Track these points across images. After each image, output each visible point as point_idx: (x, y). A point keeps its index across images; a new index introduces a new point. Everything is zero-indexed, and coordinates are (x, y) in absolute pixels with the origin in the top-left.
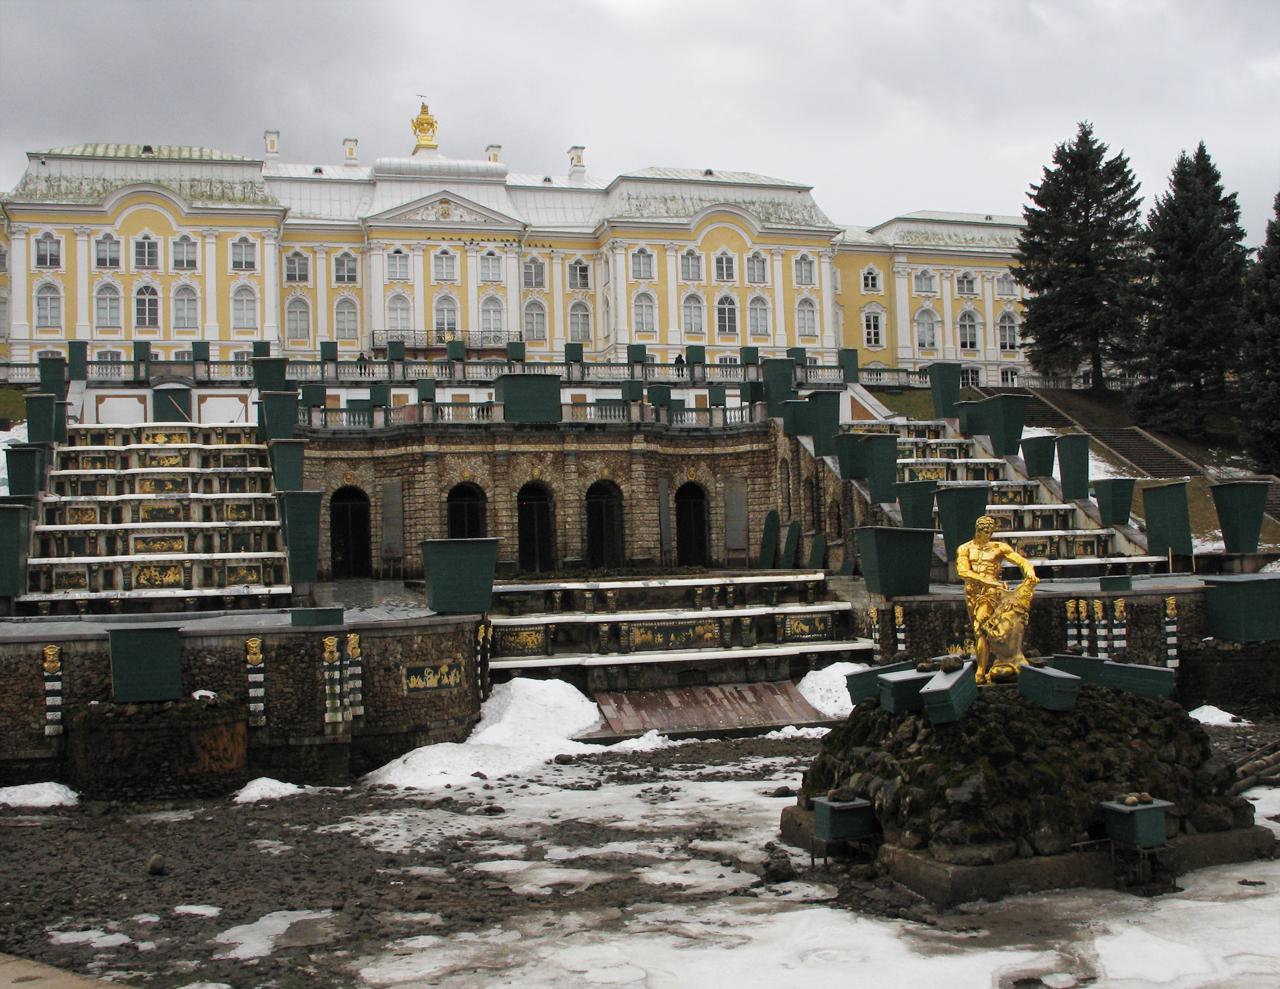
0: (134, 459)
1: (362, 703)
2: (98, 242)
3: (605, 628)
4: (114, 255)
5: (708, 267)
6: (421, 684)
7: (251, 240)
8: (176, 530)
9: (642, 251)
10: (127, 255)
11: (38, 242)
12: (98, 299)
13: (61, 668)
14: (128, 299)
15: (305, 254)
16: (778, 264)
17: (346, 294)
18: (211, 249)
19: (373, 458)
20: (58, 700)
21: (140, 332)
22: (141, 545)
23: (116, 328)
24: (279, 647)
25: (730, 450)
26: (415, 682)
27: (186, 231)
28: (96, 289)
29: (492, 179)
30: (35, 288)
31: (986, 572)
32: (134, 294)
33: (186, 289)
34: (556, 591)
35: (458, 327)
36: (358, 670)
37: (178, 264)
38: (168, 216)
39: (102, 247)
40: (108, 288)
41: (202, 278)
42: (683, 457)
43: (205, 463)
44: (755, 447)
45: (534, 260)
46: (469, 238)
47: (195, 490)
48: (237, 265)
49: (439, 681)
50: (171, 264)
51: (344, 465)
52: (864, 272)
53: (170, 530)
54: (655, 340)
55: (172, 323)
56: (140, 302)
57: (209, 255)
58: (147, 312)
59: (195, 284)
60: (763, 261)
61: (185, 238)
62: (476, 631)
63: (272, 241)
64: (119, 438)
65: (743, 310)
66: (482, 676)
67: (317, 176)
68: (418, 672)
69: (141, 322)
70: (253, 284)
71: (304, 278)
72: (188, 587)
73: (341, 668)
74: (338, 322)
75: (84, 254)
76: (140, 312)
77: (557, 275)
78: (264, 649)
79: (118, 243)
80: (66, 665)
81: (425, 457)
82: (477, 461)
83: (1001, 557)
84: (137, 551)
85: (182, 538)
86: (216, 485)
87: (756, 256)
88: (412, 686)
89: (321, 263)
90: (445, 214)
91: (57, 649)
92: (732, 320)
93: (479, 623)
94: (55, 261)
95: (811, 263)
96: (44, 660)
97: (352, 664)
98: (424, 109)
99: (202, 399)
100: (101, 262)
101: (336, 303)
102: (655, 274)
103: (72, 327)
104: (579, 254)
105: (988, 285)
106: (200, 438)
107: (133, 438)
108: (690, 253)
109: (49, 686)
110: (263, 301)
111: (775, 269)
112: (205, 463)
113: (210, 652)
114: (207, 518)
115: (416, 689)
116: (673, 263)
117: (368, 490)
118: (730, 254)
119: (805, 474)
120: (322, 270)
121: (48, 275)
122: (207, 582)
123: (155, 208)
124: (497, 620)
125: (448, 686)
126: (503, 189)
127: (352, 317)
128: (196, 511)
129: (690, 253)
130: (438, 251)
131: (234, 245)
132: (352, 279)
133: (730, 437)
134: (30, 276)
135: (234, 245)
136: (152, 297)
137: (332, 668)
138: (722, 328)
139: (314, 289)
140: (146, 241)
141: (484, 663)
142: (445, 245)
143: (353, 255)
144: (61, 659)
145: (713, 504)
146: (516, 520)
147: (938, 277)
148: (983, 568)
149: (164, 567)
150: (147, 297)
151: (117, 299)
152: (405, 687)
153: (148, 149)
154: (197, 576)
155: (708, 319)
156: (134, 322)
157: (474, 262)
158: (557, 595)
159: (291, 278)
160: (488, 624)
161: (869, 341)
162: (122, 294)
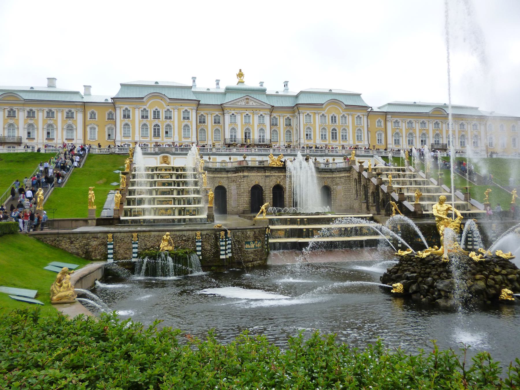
0: (155, 176)
1: (231, 252)
2: (142, 111)
3: (305, 230)
5: (328, 119)
6: (249, 247)
7: (188, 110)
8: (170, 198)
9: (308, 114)
10: (151, 115)
11: (124, 110)
14: (151, 128)
16: (350, 118)
17: (217, 127)
18: (176, 113)
20: (136, 250)
22: (158, 202)
24: (207, 234)
25: (338, 176)
26: (247, 246)
27: (168, 107)
28: (141, 125)
29: (263, 91)
30: (123, 125)
31: (443, 214)
32: (153, 127)
33: (168, 125)
35: (251, 137)
36: (230, 242)
38: (163, 103)
40: (145, 125)
41: (174, 122)
42: (323, 178)
43: (177, 178)
44: (346, 175)
45: (274, 117)
46: (254, 110)
47: (174, 186)
48: (184, 118)
49: (255, 246)
50: (164, 118)
51: (219, 179)
52: (378, 120)
53: (168, 198)
54: (312, 142)
57: (176, 115)
58: (157, 134)
59: (171, 124)
60: (346, 117)
61: (168, 110)
62: (266, 230)
64: (150, 170)
65: (339, 132)
66: (267, 245)
68: (248, 243)
69: (155, 135)
70: (189, 124)
71: (204, 122)
72: (174, 215)
73: (226, 241)
75: (137, 115)
76: (155, 132)
77: (281, 122)
78: (201, 235)
81: (244, 177)
82: (259, 178)
83: (448, 209)
84: (158, 204)
86: (181, 184)
87: (343, 116)
89: (209, 118)
90: (247, 103)
91: (136, 234)
92: (336, 136)
93: (266, 228)
94: (129, 117)
95: (361, 118)
96: (132, 237)
97: (229, 240)
98: (240, 70)
99: (174, 159)
100: (143, 117)
102: (312, 121)
103: (133, 137)
104: (288, 115)
105: (417, 124)
106: (175, 170)
107: (155, 170)
108: (323, 115)
109: (134, 246)
110: (192, 129)
111: (350, 119)
112: (177, 178)
113: (185, 236)
114: (179, 194)
115: (248, 248)
116: (317, 117)
117: (226, 187)
118: (335, 115)
119: (362, 183)
120: (209, 120)
121: (126, 121)
122: (180, 214)
124: (271, 227)
125: (257, 247)
126: (265, 96)
127: (219, 134)
128: (175, 192)
129: (323, 115)
130: (245, 114)
131: (183, 112)
133: (338, 171)
134: (121, 121)
137: (222, 241)
138: (333, 138)
139: (207, 126)
141: (267, 241)
142: (247, 112)
143: (219, 115)
144: (138, 237)
145: (332, 192)
146: (272, 197)
147: (401, 122)
148: (442, 213)
149: (167, 209)
150: (157, 128)
154: (177, 212)
155: (329, 136)
157: (256, 118)
160: (269, 228)
161: (378, 142)
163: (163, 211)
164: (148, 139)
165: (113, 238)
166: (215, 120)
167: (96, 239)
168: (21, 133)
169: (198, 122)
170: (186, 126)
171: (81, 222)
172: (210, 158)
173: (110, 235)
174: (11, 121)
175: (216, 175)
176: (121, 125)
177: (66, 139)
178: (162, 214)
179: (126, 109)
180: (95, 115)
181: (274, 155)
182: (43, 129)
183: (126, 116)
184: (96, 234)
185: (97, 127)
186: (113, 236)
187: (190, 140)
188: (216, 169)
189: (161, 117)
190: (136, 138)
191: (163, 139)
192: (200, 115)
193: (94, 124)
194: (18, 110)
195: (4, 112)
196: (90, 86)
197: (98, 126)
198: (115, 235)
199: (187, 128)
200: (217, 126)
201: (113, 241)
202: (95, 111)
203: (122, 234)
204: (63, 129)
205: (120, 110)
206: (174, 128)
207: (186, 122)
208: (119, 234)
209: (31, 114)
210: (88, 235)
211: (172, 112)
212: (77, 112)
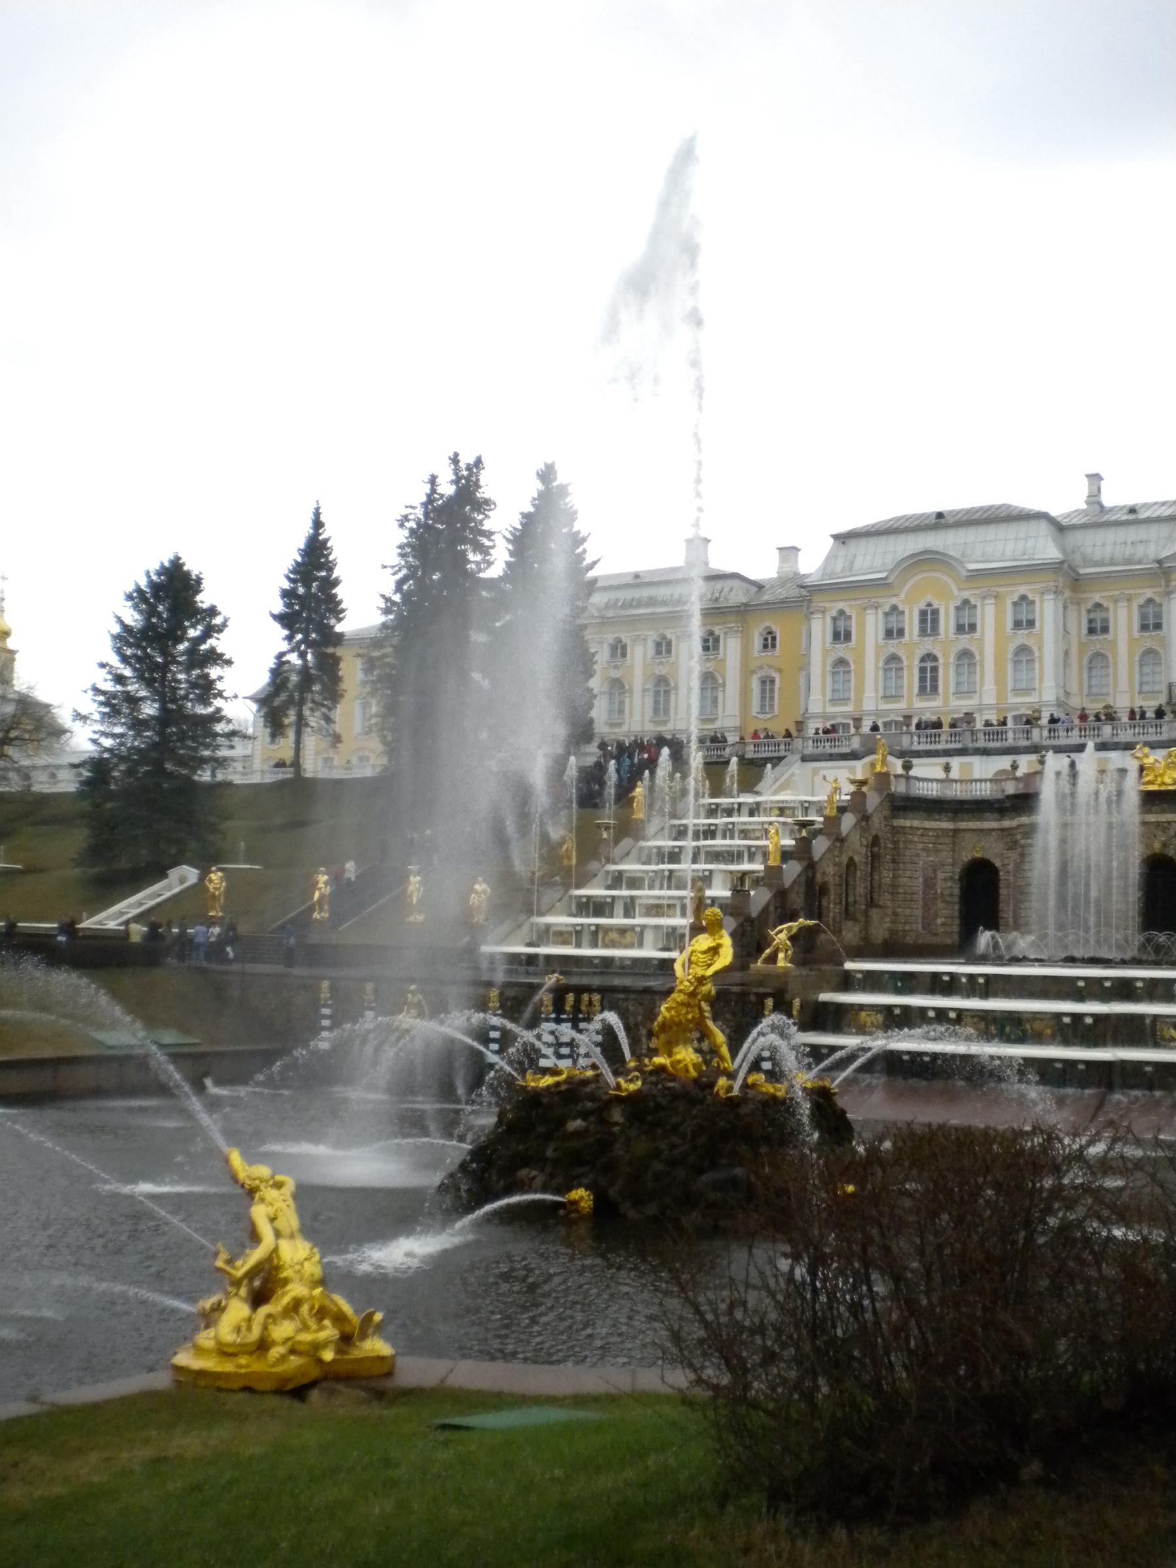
2: (886, 614)
4: (900, 626)
7: (1031, 596)
10: (912, 624)
12: (885, 670)
13: (375, 1001)
14: (910, 667)
15: (1105, 604)
19: (1002, 830)
23: (896, 697)
27: (966, 594)
30: (830, 660)
32: (917, 662)
34: (963, 974)
37: (960, 629)
40: (894, 658)
41: (982, 639)
48: (1018, 624)
55: (952, 689)
56: (923, 670)
57: (987, 616)
58: (929, 682)
59: (974, 649)
63: (1052, 596)
67: (1132, 517)
69: (922, 689)
70: (1031, 642)
71: (1105, 630)
72: (641, 945)
74: (1142, 674)
76: (922, 679)
79: (903, 613)
84: (641, 915)
85: (674, 906)
94: (848, 636)
100: (889, 633)
101: (1137, 659)
103: (859, 701)
117: (998, 864)
120: (1124, 620)
121: (841, 650)
123: (935, 574)
132: (1158, 626)
134: (826, 652)
135: (1015, 604)
139: (1114, 643)
149: (623, 931)
150: (929, 665)
151: (902, 669)
152: (645, 1047)
153: (940, 515)
156: (916, 690)
158: (541, 959)
159: (1092, 631)
162: (905, 663)
163: (614, 936)
165: (331, 992)
166: (1143, 616)
169: (1084, 631)
170: (1023, 650)
172: (947, 768)
175: (963, 825)
176: (824, 665)
178: (613, 944)
179: (842, 612)
180: (774, 639)
181: (1153, 746)
182: (644, 691)
183: (841, 635)
185: (776, 676)
187: (1032, 699)
188: (962, 803)
190: (865, 701)
191: (946, 701)
192: (1090, 605)
193: (770, 667)
196: (798, 550)
197: (780, 671)
199: (1024, 658)
200: (1149, 640)
201: (331, 998)
202: (774, 628)
205: (824, 618)
206: (982, 662)
207: (1022, 637)
211: (979, 608)
212: (726, 633)
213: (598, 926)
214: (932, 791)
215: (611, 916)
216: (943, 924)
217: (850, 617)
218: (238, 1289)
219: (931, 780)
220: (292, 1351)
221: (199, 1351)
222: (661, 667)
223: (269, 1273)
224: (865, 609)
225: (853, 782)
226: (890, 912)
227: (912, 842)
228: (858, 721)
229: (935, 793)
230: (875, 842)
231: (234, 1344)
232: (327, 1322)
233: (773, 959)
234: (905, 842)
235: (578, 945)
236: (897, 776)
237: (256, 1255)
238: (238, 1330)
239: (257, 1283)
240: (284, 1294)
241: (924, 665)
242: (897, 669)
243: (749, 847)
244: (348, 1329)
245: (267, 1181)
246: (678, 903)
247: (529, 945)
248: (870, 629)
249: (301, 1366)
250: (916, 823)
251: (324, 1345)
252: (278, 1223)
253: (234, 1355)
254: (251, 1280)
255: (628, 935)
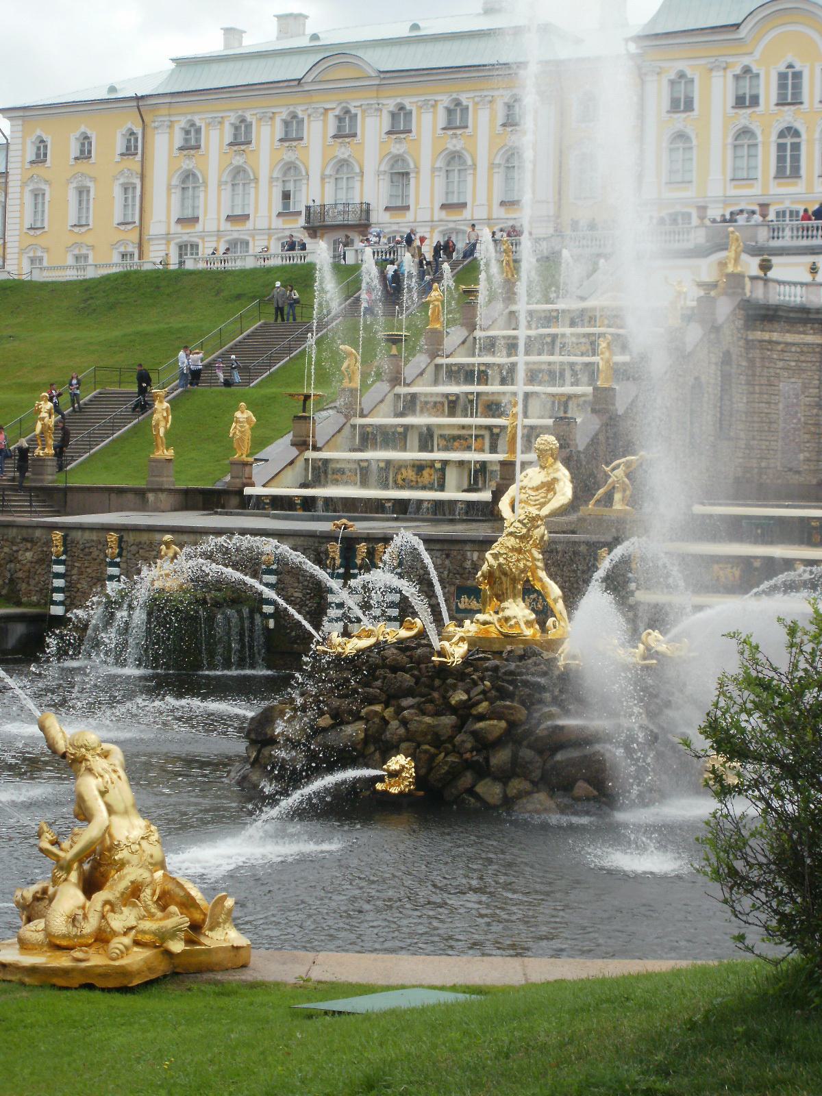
2: (737, 77)
4: (754, 92)
10: (768, 91)
21: (779, 185)
22: (443, 443)
23: (751, 179)
32: (774, 137)
39: (741, 83)
40: (745, 132)
56: (781, 147)
58: (789, 164)
69: (780, 174)
72: (442, 488)
76: (781, 159)
79: (757, 76)
80: (124, 553)
85: (482, 437)
88: (461, 606)
94: (689, 106)
100: (740, 102)
121: (680, 121)
136: (795, 140)
140: (790, 71)
149: (419, 467)
150: (789, 141)
151: (756, 145)
162: (760, 138)
163: (410, 474)
164: (756, 190)
165: (65, 545)
167: (29, 545)
168: (372, 191)
171: (130, 496)
172: (814, 270)
173: (58, 535)
174: (342, 152)
177: (502, 203)
179: (682, 75)
182: (433, 170)
184: (30, 531)
186: (65, 538)
189: (805, 97)
194: (364, 111)
195: (325, 122)
198: (77, 535)
201: (65, 552)
203: (87, 535)
204: (492, 166)
208: (80, 533)
209: (400, 124)
210: (15, 530)
213: (388, 462)
214: (795, 297)
215: (404, 449)
216: (808, 460)
217: (692, 81)
218: (68, 873)
219: (795, 284)
220: (137, 943)
221: (24, 945)
222: (454, 141)
223: (101, 854)
224: (711, 70)
225: (700, 285)
226: (742, 444)
227: (770, 359)
228: (702, 209)
229: (798, 299)
230: (726, 359)
231: (64, 936)
232: (173, 908)
233: (608, 499)
234: (763, 359)
235: (364, 483)
236: (753, 278)
237: (91, 832)
238: (73, 920)
239: (86, 867)
240: (121, 878)
241: (781, 141)
242: (749, 146)
243: (572, 365)
244: (198, 916)
245: (93, 749)
246: (487, 434)
247: (304, 485)
248: (717, 92)
249: (146, 960)
250: (775, 336)
251: (172, 934)
252: (108, 797)
253: (69, 948)
254: (81, 862)
255: (426, 473)
